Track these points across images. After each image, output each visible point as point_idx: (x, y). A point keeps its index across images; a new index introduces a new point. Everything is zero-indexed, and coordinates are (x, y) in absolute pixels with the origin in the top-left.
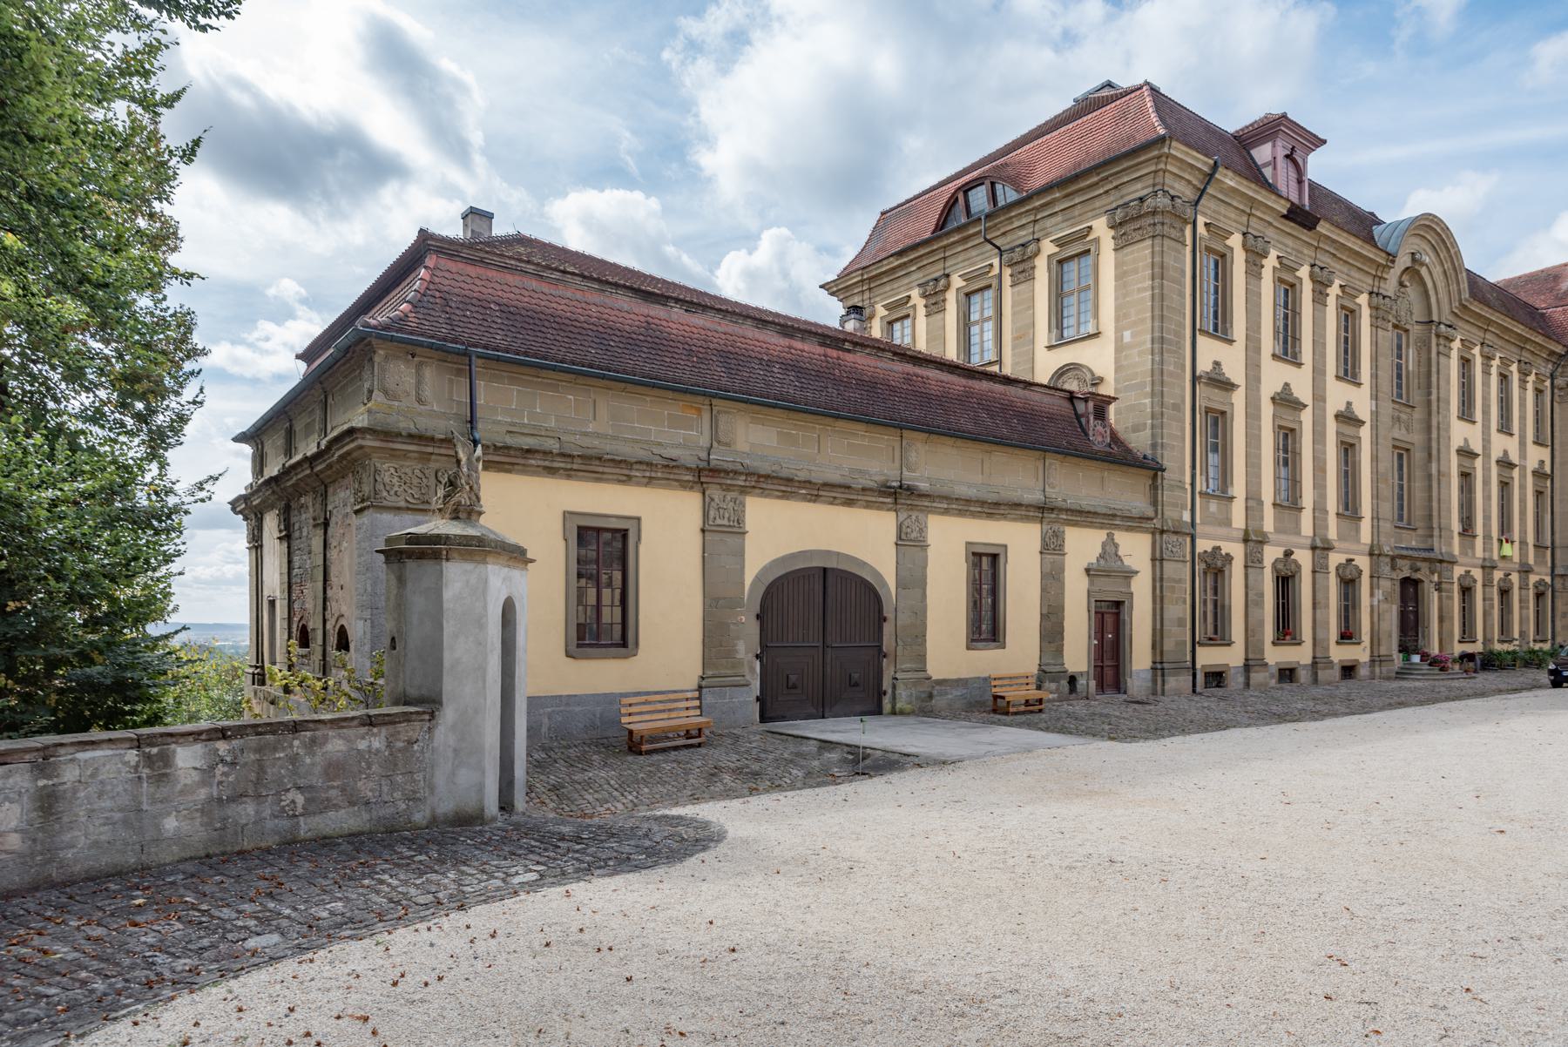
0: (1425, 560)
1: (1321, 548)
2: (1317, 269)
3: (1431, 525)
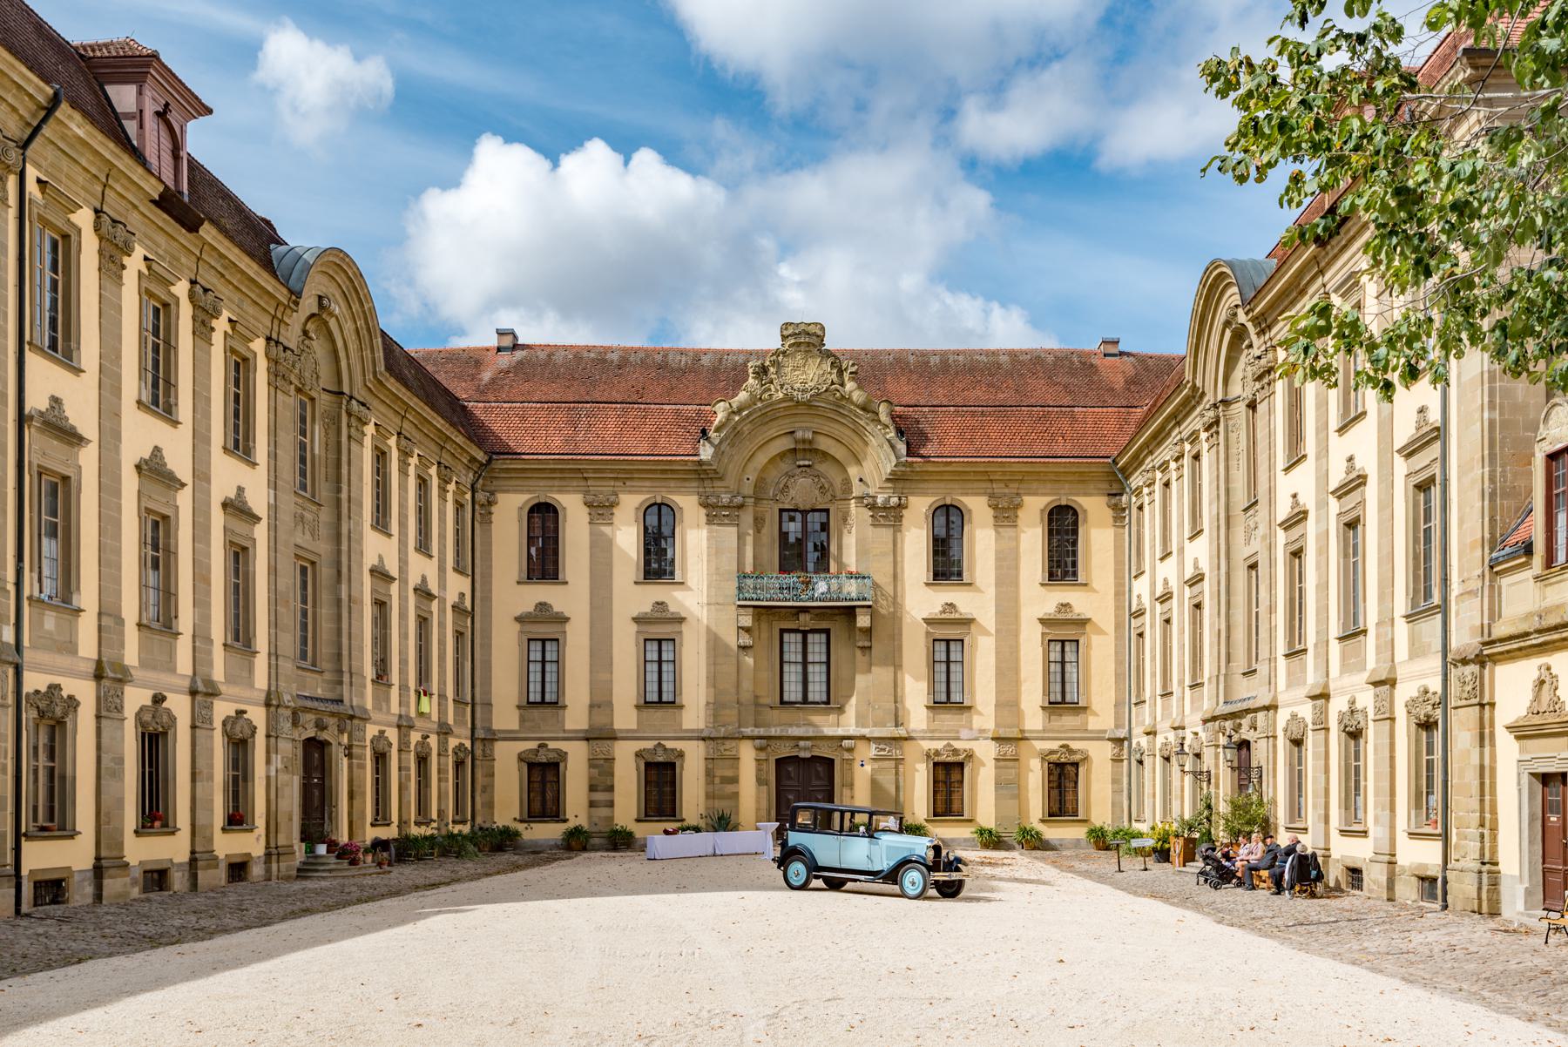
0: (333, 714)
1: (202, 692)
2: (198, 288)
3: (340, 671)
